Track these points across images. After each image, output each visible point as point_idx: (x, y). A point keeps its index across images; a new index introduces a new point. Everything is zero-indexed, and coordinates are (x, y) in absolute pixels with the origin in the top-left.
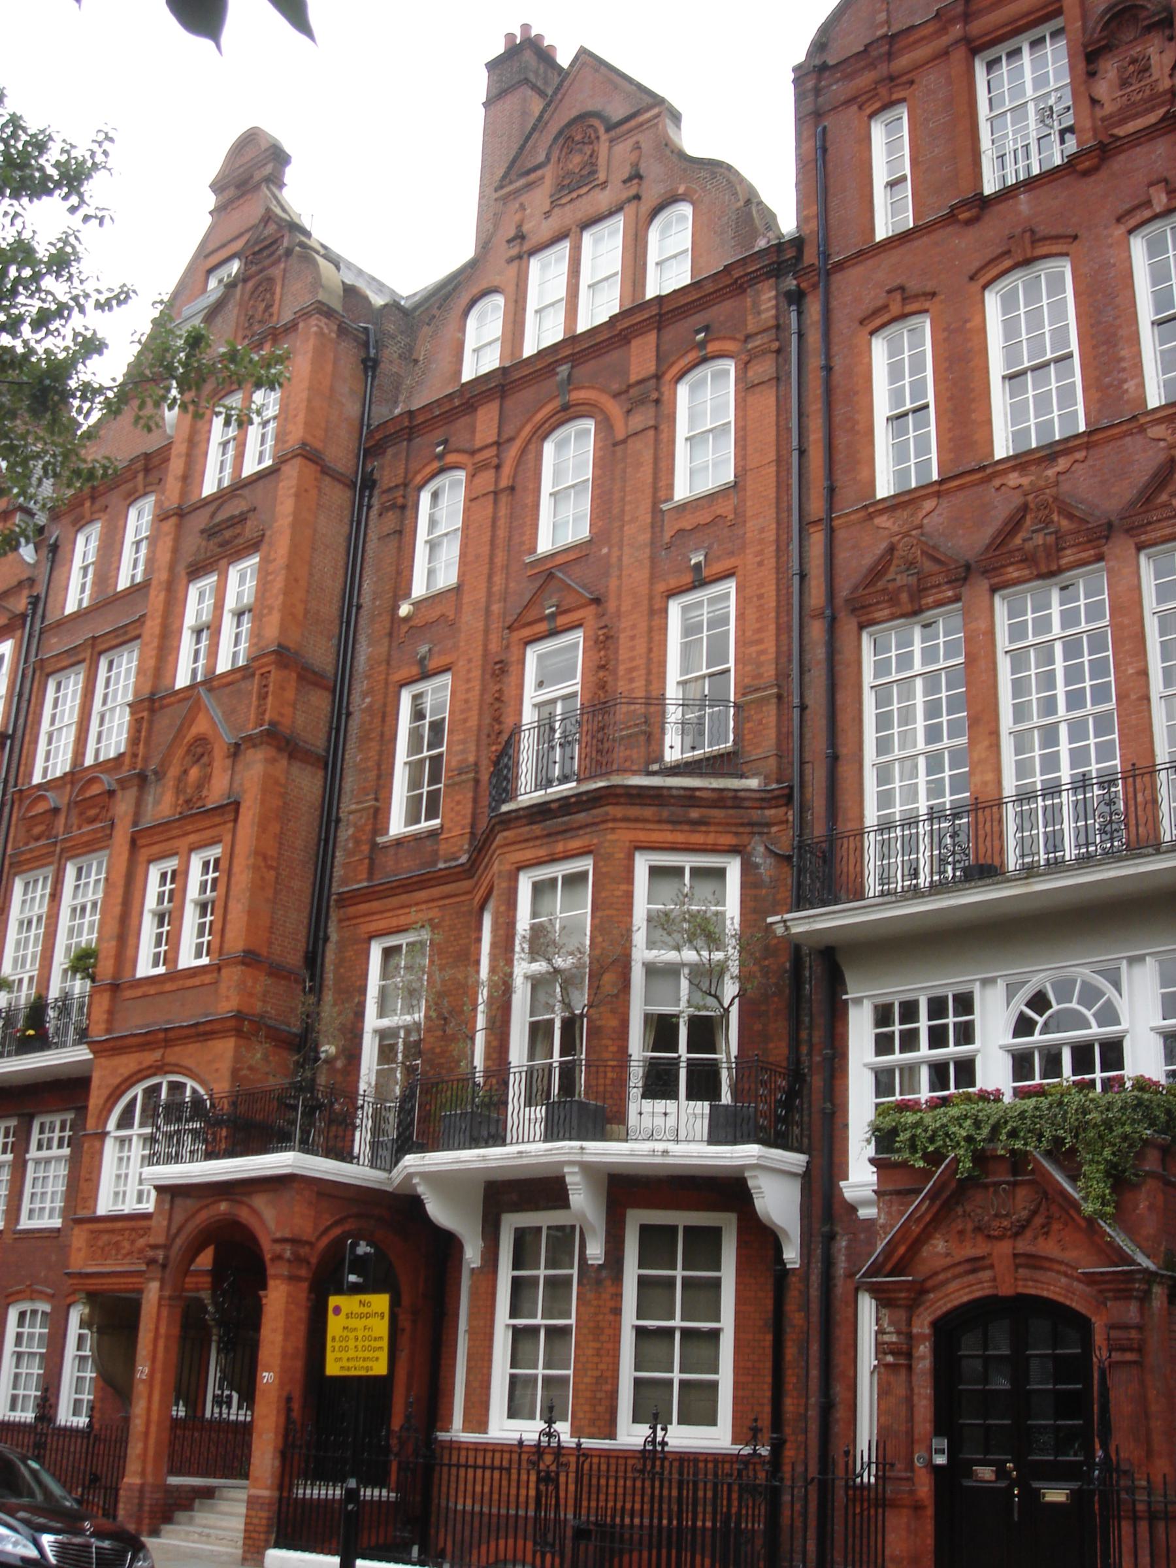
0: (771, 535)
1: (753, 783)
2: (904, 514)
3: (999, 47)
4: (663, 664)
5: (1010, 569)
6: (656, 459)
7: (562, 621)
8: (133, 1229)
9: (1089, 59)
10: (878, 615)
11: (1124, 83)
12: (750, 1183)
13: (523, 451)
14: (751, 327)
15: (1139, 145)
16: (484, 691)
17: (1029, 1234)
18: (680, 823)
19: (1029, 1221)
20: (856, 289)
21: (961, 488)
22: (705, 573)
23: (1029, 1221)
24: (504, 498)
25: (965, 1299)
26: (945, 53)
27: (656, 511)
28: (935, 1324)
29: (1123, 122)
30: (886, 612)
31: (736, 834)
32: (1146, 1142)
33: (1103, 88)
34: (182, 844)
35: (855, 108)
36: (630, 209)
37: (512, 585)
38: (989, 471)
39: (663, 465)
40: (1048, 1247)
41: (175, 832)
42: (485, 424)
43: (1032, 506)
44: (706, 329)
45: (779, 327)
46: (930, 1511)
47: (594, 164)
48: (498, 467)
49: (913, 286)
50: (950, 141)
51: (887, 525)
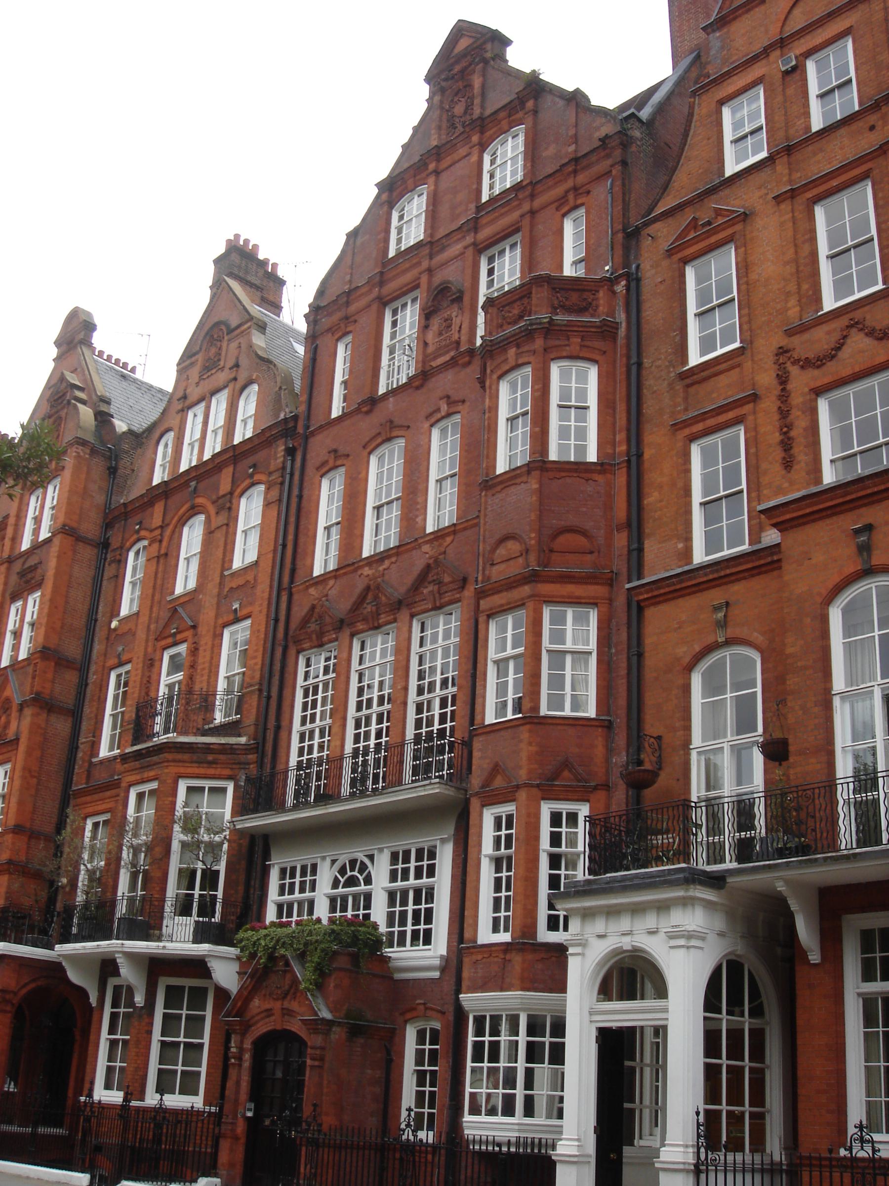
0: (266, 595)
1: (243, 740)
2: (320, 587)
3: (396, 302)
4: (218, 666)
5: (358, 624)
6: (226, 544)
9: (427, 315)
10: (305, 646)
11: (440, 334)
12: (209, 965)
13: (173, 532)
14: (272, 468)
15: (441, 372)
16: (143, 675)
17: (289, 998)
18: (202, 763)
19: (288, 991)
20: (319, 448)
21: (345, 574)
22: (239, 614)
23: (288, 991)
24: (162, 561)
25: (265, 1030)
26: (369, 306)
27: (222, 576)
28: (255, 1043)
29: (435, 358)
30: (308, 644)
31: (232, 769)
32: (335, 953)
33: (430, 337)
35: (330, 334)
36: (231, 385)
37: (161, 613)
38: (356, 565)
39: (229, 547)
40: (295, 1006)
42: (156, 515)
43: (372, 587)
44: (254, 466)
45: (284, 468)
46: (243, 1140)
47: (220, 354)
48: (161, 541)
49: (342, 450)
50: (368, 361)
51: (313, 593)
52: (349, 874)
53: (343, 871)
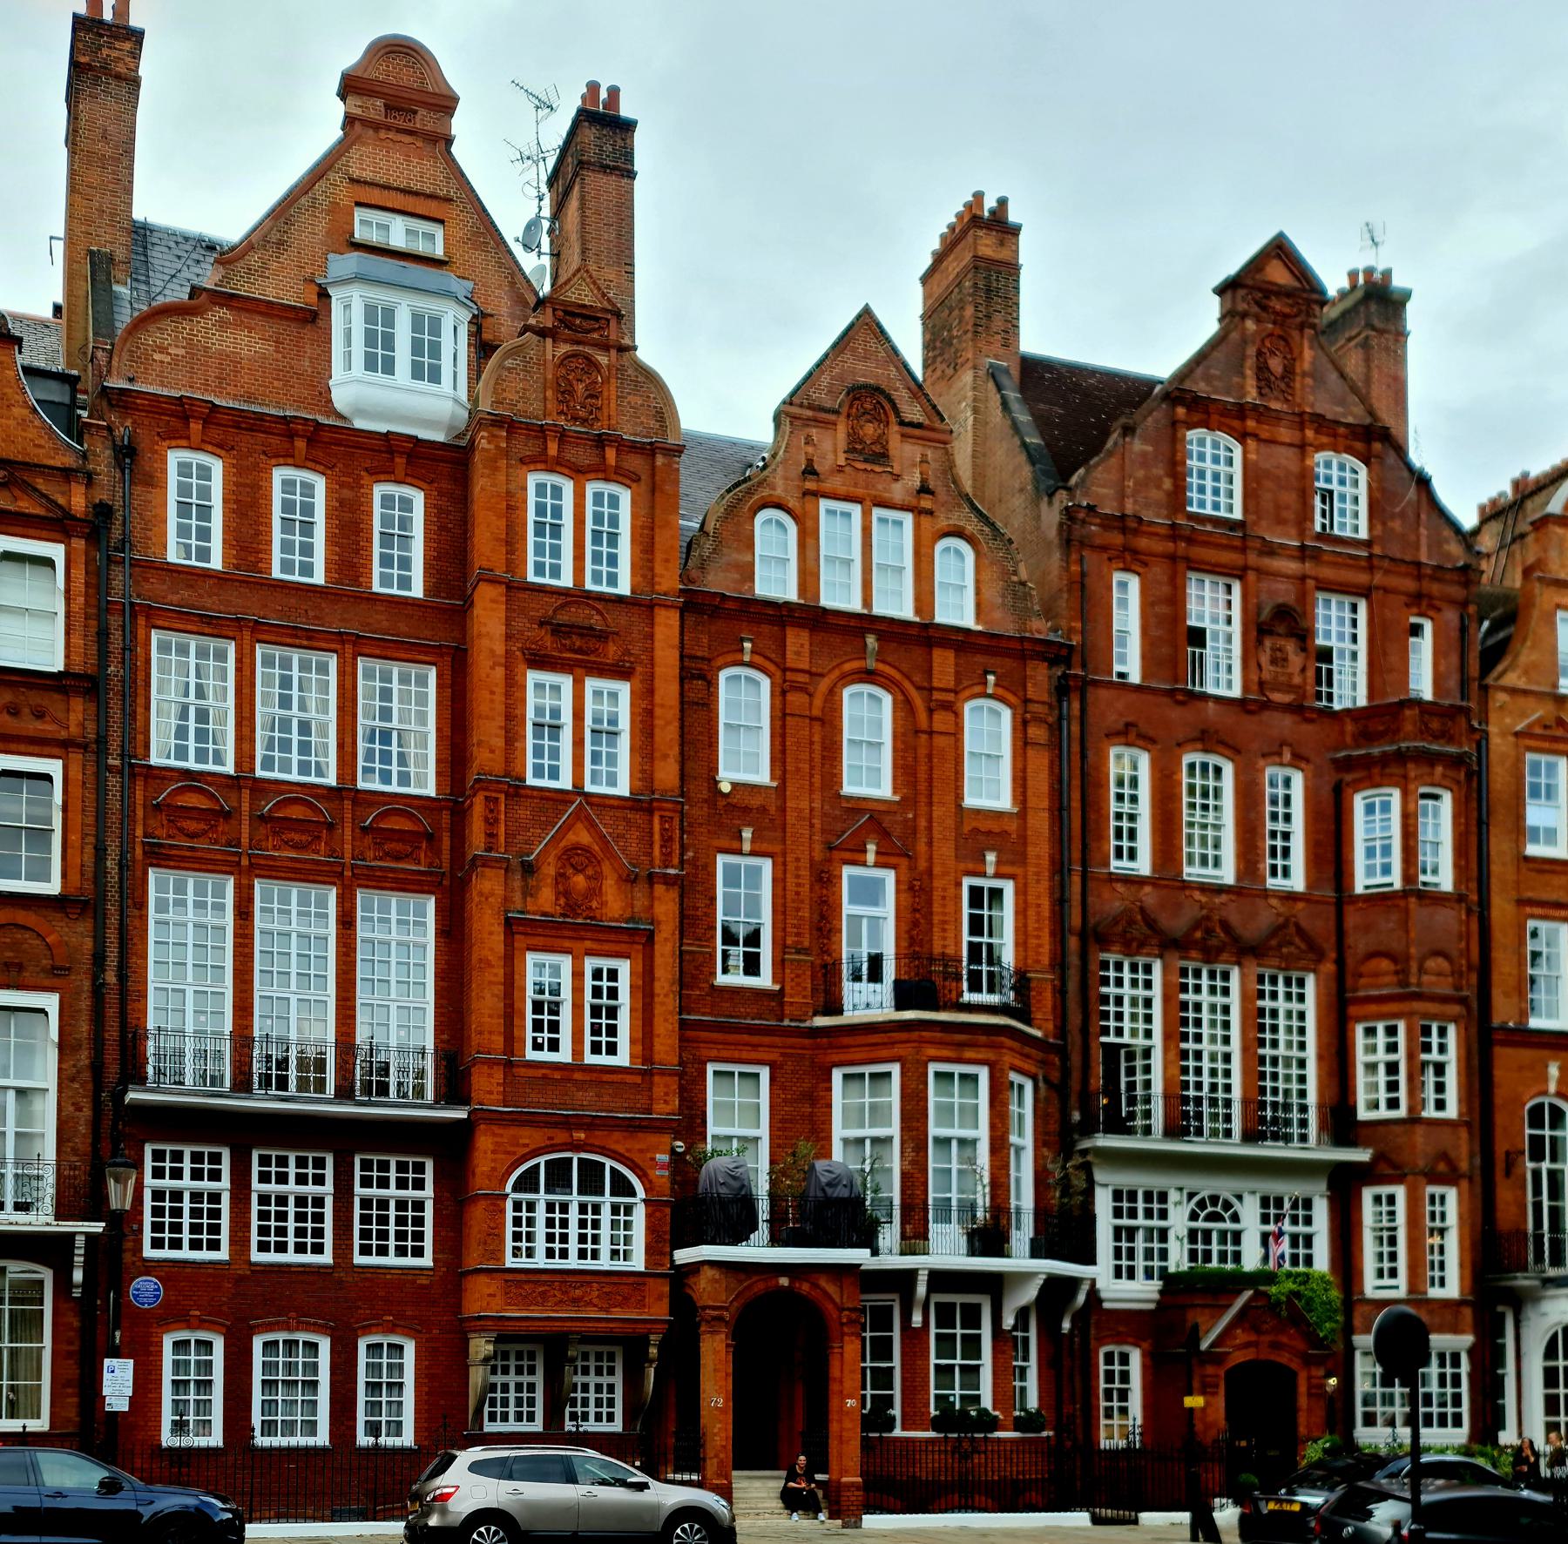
1: (1038, 1033)
34: (579, 946)
52: (1210, 1209)
53: (1201, 1204)
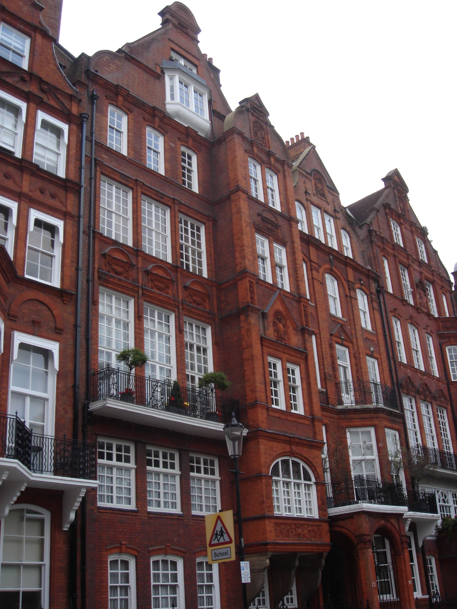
7: (345, 343)
8: (295, 524)
41: (281, 349)
